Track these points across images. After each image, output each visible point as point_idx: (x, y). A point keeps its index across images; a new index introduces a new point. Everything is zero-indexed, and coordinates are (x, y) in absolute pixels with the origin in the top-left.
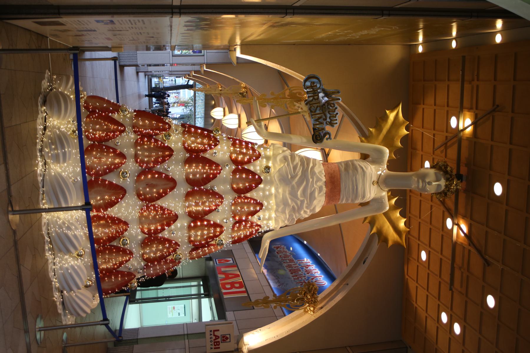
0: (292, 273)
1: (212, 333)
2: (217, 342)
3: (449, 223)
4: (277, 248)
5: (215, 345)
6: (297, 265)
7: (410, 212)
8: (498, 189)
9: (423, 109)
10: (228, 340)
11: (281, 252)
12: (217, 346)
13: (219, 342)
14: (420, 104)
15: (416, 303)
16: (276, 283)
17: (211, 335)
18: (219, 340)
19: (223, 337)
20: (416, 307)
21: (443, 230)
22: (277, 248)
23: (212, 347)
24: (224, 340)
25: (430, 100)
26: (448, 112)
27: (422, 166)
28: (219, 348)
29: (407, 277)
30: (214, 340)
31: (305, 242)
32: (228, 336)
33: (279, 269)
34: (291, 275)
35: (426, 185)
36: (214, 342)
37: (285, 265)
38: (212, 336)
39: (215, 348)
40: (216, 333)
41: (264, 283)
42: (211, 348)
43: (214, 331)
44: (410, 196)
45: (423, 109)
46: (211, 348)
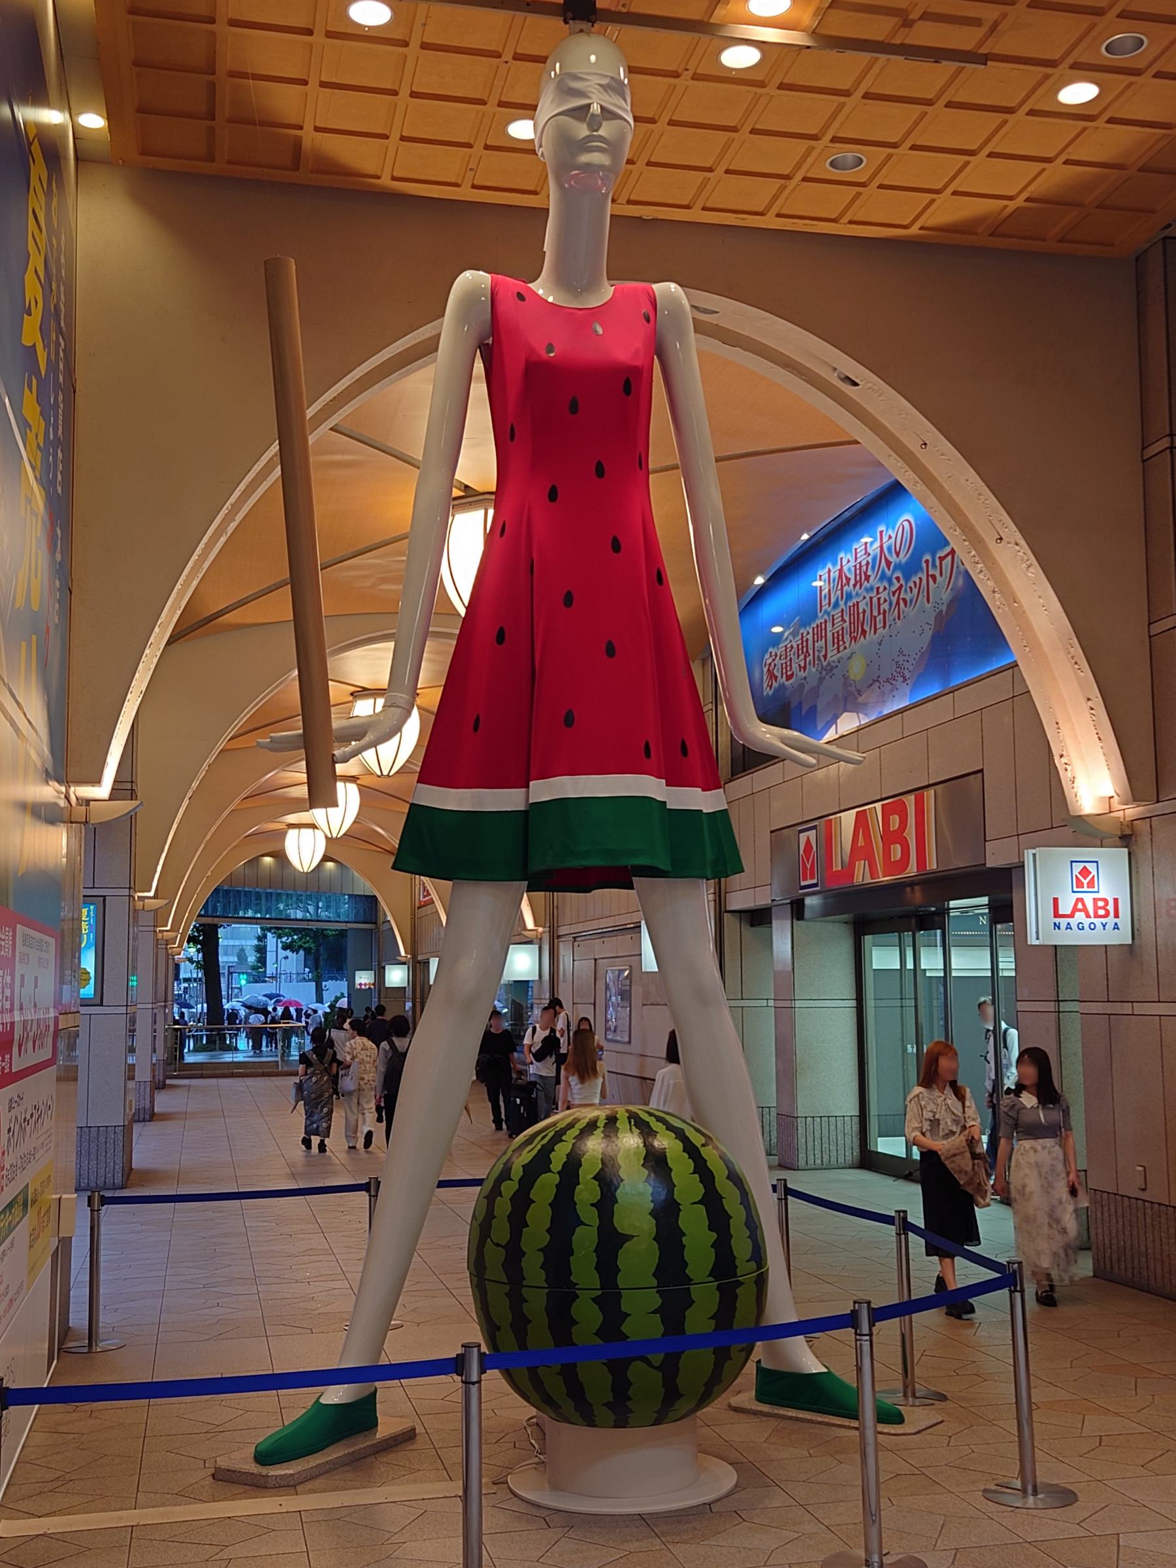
0: (864, 632)
1: (1063, 922)
2: (1096, 908)
5: (1107, 915)
10: (1091, 867)
12: (1111, 907)
13: (1095, 900)
14: (298, 144)
17: (1069, 927)
18: (1089, 900)
19: (1080, 884)
23: (1110, 926)
24: (1091, 884)
26: (330, 35)
27: (526, 149)
28: (1116, 900)
30: (1088, 916)
32: (1078, 868)
34: (870, 636)
36: (1096, 916)
38: (1073, 922)
39: (1116, 916)
40: (1065, 909)
41: (891, 730)
42: (1116, 927)
43: (1057, 915)
46: (1116, 927)
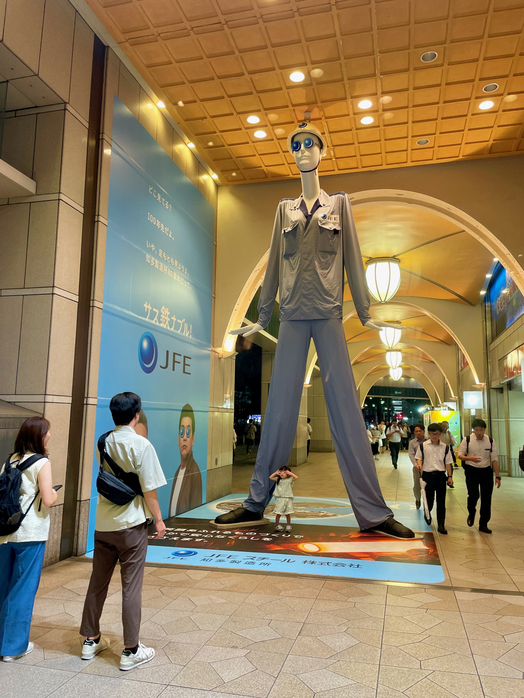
3: (367, 121)
4: (499, 308)
6: (510, 284)
7: (382, 165)
8: (297, 77)
9: (266, 166)
11: (501, 303)
15: (488, 141)
16: (522, 308)
20: (494, 140)
21: (378, 126)
22: (499, 308)
25: (255, 161)
29: (461, 157)
31: (489, 276)
33: (512, 306)
35: (305, 156)
37: (510, 299)
44: (363, 167)
45: (266, 166)
